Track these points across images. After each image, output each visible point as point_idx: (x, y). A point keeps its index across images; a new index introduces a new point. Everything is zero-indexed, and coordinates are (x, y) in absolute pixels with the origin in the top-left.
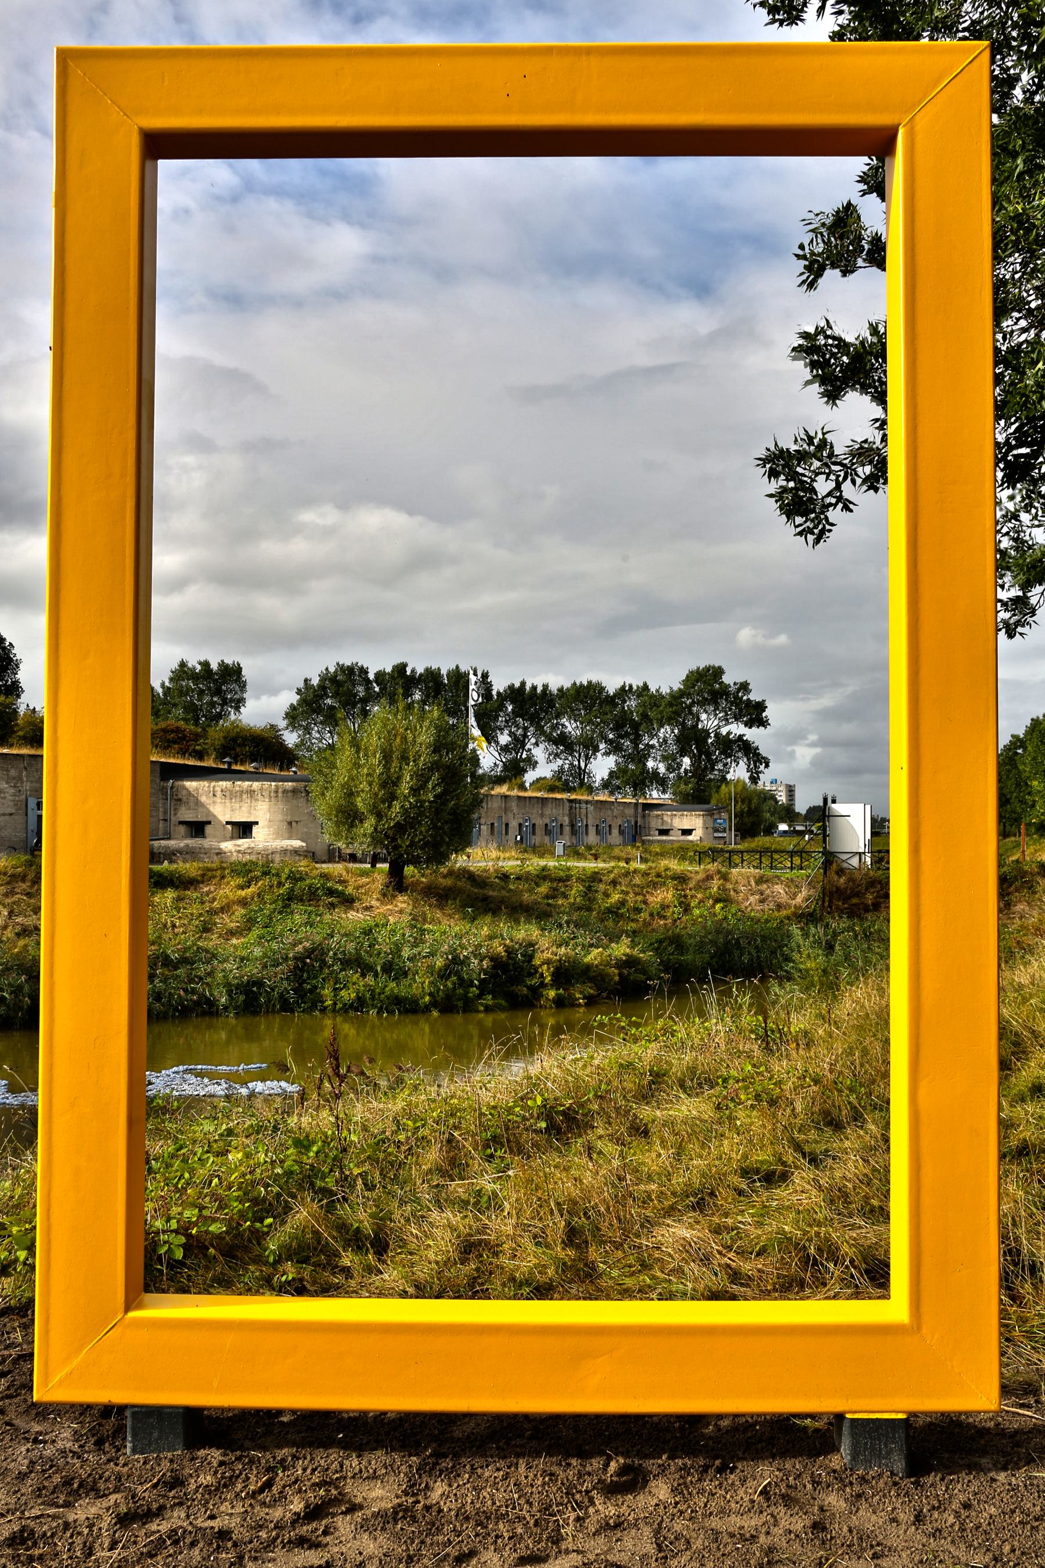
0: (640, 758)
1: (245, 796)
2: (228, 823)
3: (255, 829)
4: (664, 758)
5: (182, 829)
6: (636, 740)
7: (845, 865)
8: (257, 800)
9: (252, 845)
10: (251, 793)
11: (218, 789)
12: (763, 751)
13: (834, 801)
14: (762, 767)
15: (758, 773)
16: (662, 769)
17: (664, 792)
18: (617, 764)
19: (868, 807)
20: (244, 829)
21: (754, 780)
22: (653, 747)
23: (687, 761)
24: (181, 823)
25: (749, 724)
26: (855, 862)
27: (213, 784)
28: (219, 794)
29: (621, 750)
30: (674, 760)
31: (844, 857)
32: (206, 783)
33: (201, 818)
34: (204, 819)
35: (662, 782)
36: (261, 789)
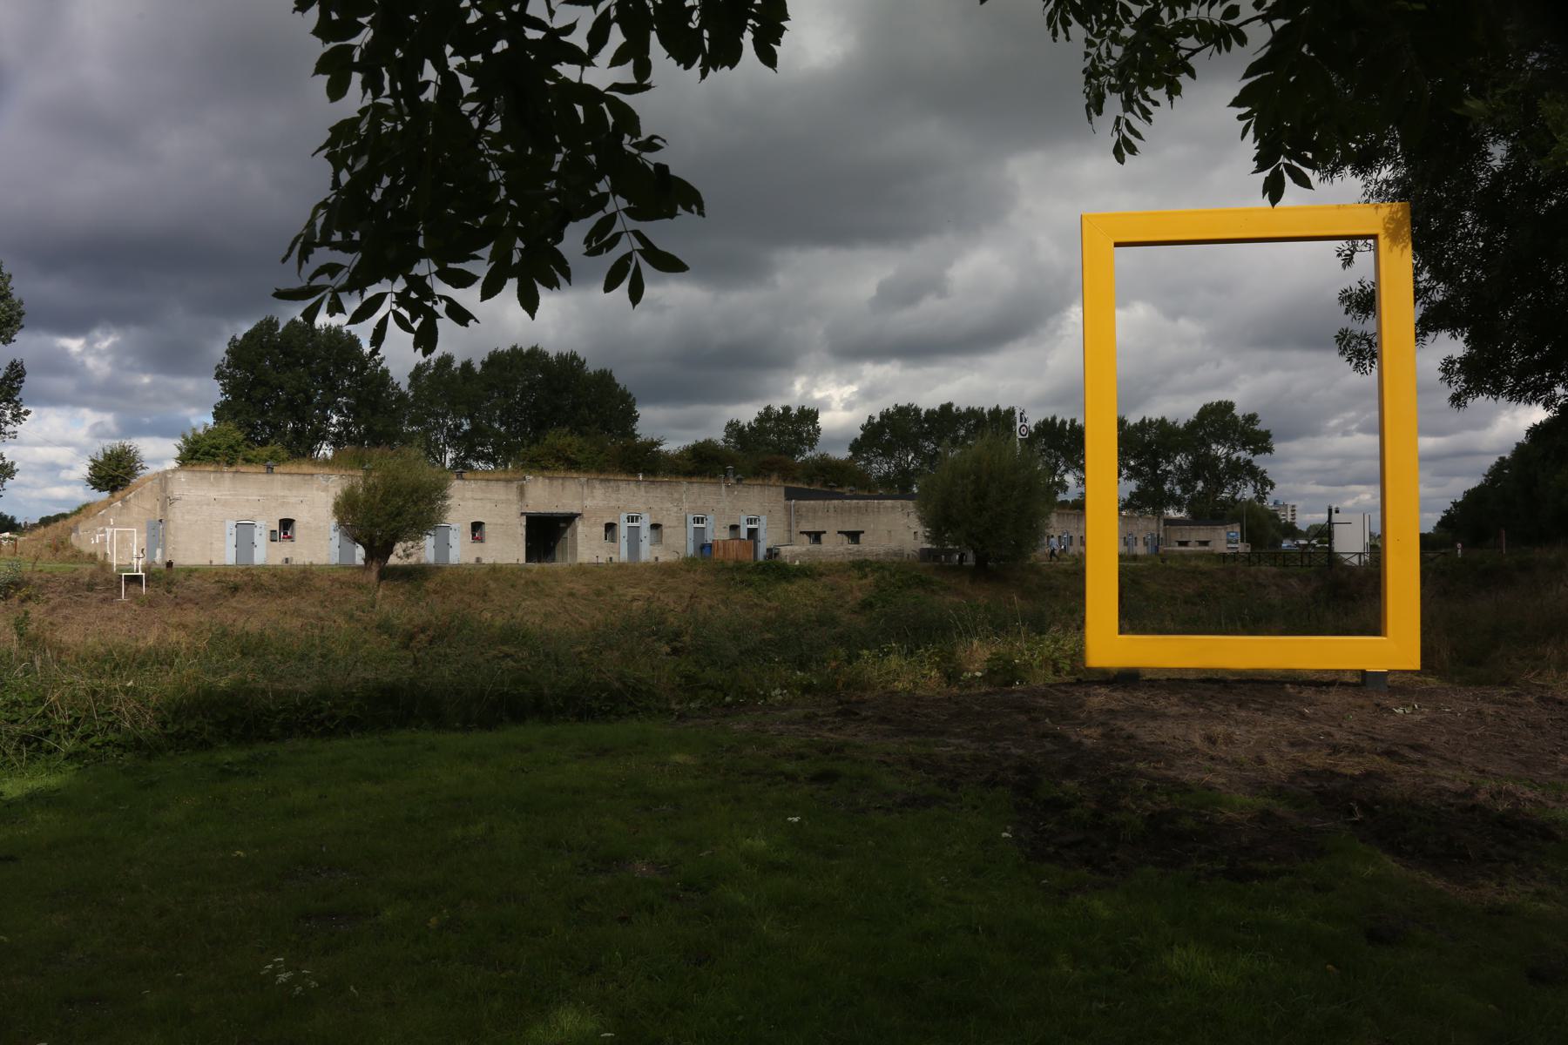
0: (1159, 481)
1: (853, 511)
2: (839, 532)
3: (861, 536)
4: (1180, 482)
5: (805, 537)
6: (1156, 465)
7: (1347, 563)
8: (863, 514)
9: (861, 549)
10: (858, 510)
11: (831, 506)
12: (1269, 476)
13: (1337, 512)
14: (1268, 489)
15: (1264, 494)
16: (1178, 491)
17: (1180, 511)
18: (1138, 487)
19: (1367, 517)
20: (854, 536)
21: (1261, 499)
22: (1170, 472)
23: (1200, 485)
24: (801, 533)
25: (1255, 452)
26: (1355, 560)
27: (827, 502)
28: (832, 510)
29: (1142, 475)
30: (1189, 484)
31: (1346, 557)
32: (821, 502)
33: (817, 529)
34: (821, 530)
35: (1177, 503)
36: (867, 506)
